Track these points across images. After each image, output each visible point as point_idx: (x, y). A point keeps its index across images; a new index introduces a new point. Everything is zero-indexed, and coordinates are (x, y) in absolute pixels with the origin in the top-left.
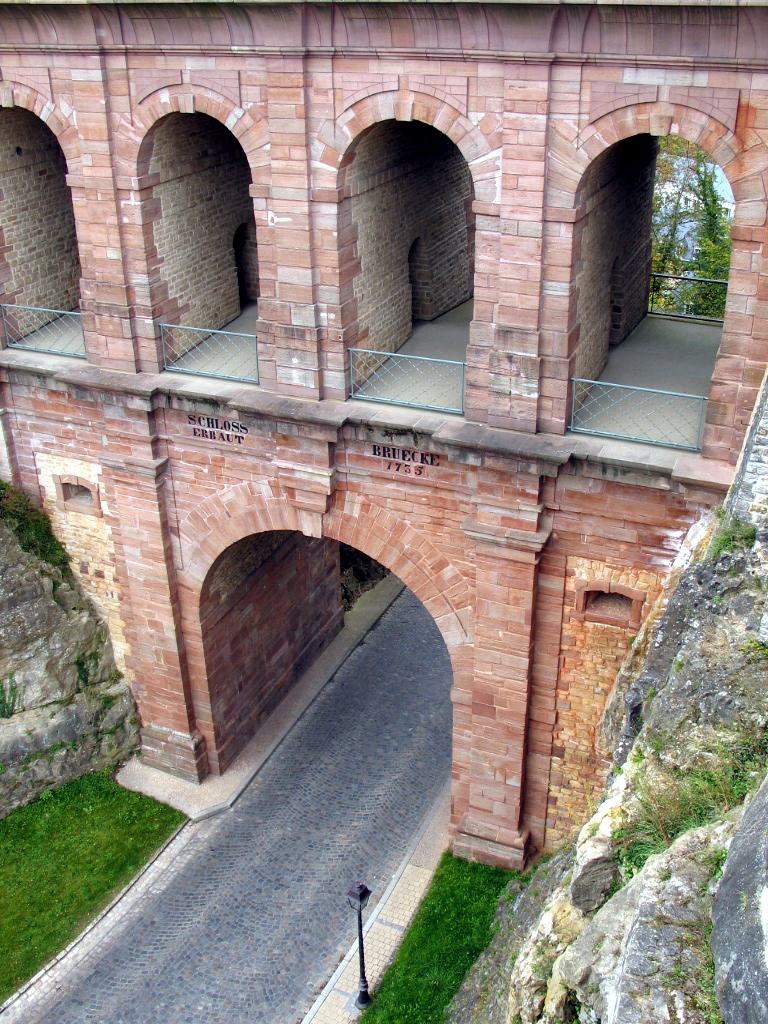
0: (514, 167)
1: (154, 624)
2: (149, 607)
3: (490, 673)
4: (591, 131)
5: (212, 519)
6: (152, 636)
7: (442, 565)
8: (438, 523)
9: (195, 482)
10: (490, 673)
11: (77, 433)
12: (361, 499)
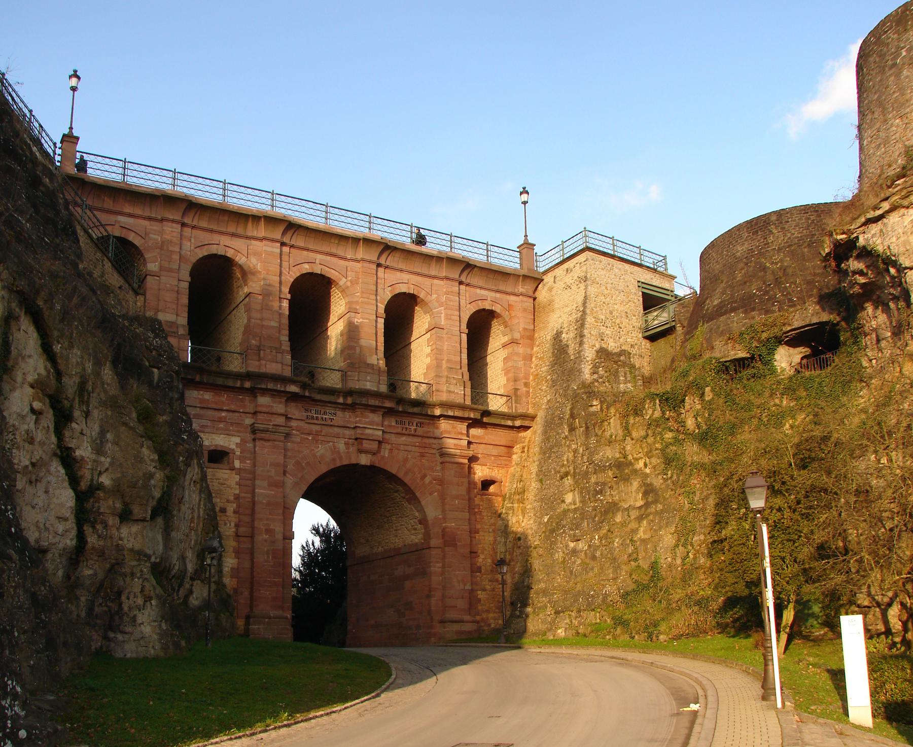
0: (450, 312)
1: (269, 531)
2: (267, 519)
3: (453, 524)
4: (469, 306)
5: (308, 463)
6: (266, 541)
7: (424, 476)
8: (422, 455)
9: (300, 443)
10: (453, 524)
11: (228, 418)
12: (389, 447)
